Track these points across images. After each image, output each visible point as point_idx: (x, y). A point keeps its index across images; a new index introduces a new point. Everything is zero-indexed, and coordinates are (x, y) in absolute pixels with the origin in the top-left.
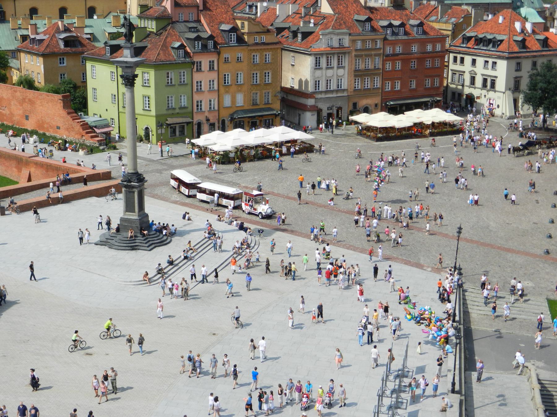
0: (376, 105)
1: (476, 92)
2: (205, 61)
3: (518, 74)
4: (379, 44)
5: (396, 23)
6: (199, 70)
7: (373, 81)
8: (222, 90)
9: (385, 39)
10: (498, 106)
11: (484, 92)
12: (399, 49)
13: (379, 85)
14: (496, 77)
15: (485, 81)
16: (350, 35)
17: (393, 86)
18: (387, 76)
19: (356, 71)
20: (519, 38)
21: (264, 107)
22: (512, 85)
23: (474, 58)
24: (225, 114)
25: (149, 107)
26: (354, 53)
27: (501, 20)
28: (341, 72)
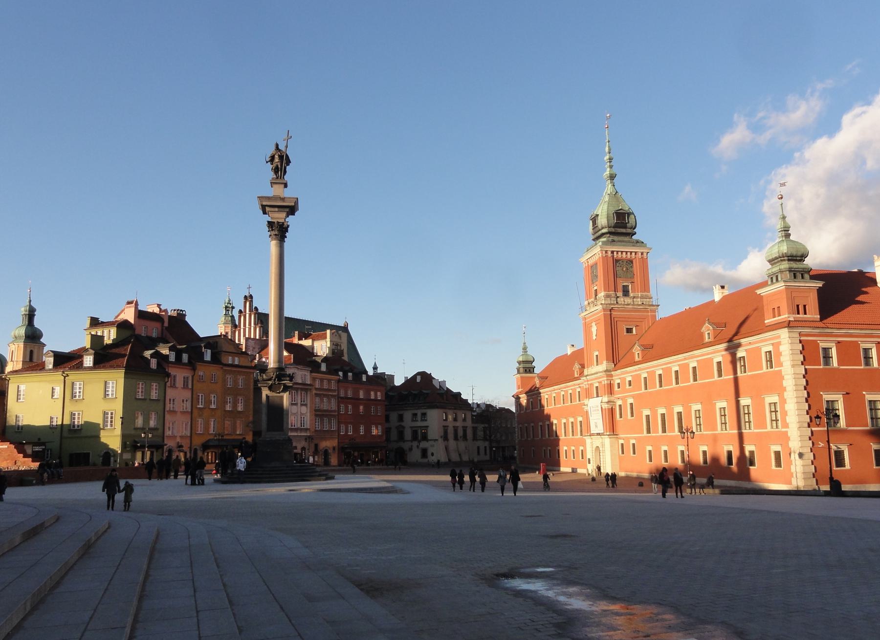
0: (334, 448)
1: (406, 446)
2: (180, 374)
3: (445, 424)
4: (333, 386)
5: (347, 368)
6: (173, 386)
7: (330, 422)
8: (195, 412)
9: (339, 381)
10: (432, 454)
11: (415, 444)
12: (350, 394)
13: (334, 428)
14: (427, 427)
15: (415, 433)
16: (311, 372)
17: (347, 431)
18: (341, 420)
19: (316, 411)
20: (442, 392)
21: (237, 437)
22: (442, 434)
23: (401, 412)
24: (198, 442)
25: (111, 425)
26: (314, 392)
27: (419, 379)
28: (304, 409)
